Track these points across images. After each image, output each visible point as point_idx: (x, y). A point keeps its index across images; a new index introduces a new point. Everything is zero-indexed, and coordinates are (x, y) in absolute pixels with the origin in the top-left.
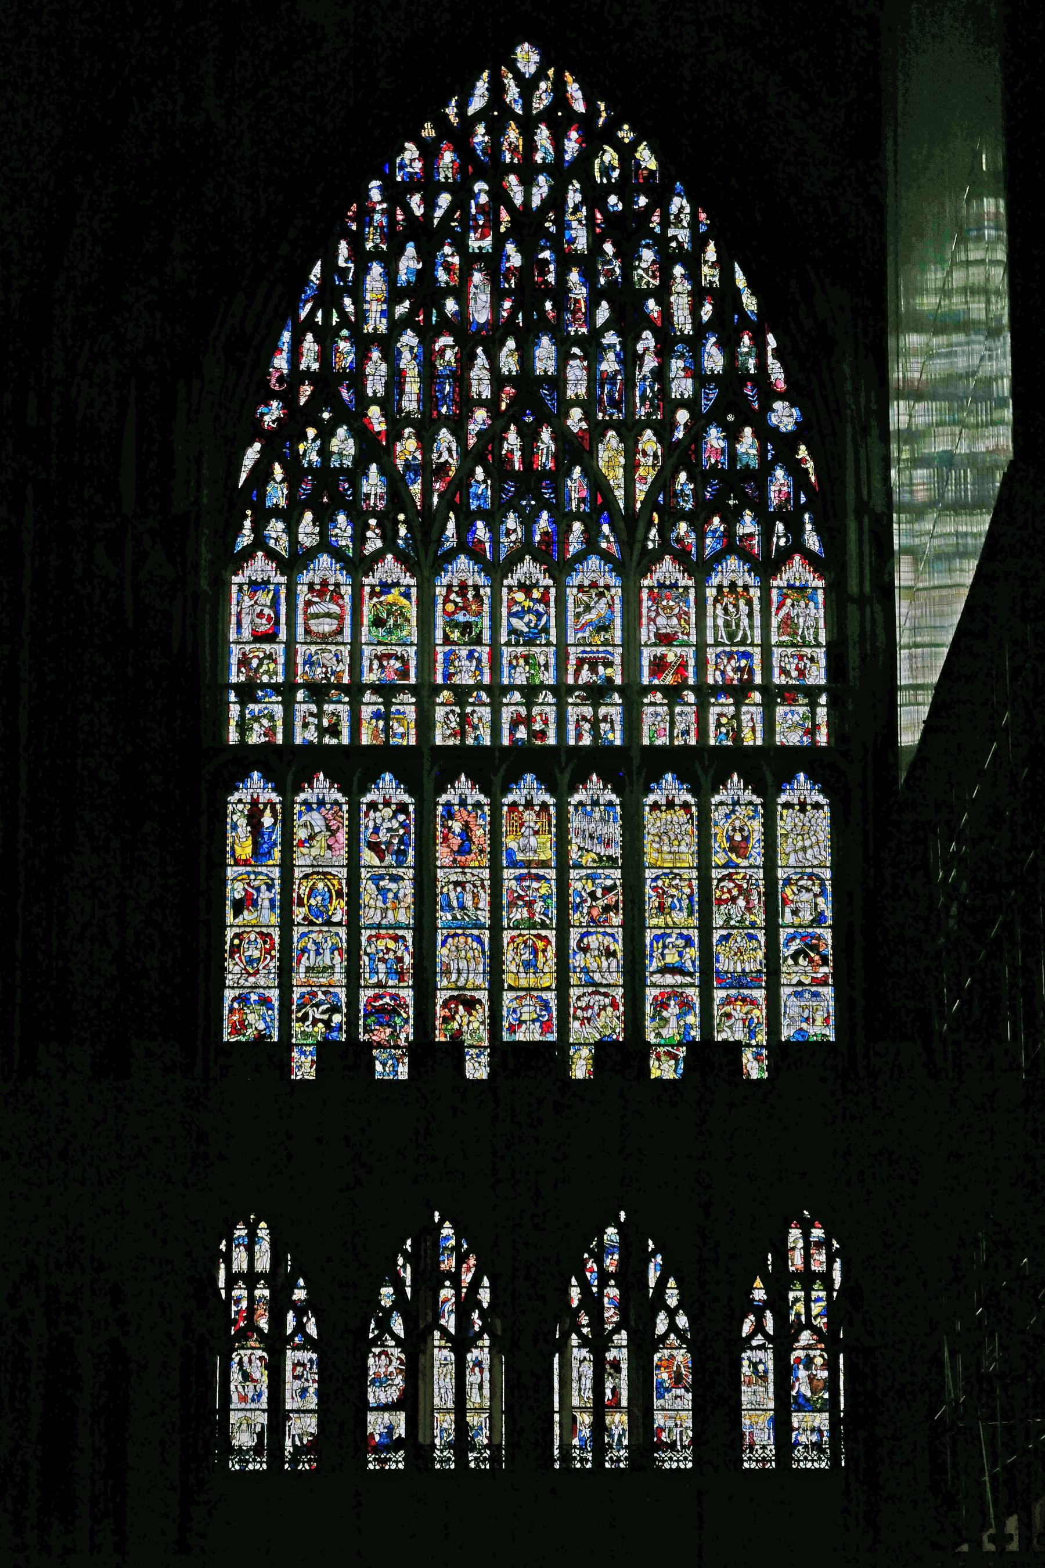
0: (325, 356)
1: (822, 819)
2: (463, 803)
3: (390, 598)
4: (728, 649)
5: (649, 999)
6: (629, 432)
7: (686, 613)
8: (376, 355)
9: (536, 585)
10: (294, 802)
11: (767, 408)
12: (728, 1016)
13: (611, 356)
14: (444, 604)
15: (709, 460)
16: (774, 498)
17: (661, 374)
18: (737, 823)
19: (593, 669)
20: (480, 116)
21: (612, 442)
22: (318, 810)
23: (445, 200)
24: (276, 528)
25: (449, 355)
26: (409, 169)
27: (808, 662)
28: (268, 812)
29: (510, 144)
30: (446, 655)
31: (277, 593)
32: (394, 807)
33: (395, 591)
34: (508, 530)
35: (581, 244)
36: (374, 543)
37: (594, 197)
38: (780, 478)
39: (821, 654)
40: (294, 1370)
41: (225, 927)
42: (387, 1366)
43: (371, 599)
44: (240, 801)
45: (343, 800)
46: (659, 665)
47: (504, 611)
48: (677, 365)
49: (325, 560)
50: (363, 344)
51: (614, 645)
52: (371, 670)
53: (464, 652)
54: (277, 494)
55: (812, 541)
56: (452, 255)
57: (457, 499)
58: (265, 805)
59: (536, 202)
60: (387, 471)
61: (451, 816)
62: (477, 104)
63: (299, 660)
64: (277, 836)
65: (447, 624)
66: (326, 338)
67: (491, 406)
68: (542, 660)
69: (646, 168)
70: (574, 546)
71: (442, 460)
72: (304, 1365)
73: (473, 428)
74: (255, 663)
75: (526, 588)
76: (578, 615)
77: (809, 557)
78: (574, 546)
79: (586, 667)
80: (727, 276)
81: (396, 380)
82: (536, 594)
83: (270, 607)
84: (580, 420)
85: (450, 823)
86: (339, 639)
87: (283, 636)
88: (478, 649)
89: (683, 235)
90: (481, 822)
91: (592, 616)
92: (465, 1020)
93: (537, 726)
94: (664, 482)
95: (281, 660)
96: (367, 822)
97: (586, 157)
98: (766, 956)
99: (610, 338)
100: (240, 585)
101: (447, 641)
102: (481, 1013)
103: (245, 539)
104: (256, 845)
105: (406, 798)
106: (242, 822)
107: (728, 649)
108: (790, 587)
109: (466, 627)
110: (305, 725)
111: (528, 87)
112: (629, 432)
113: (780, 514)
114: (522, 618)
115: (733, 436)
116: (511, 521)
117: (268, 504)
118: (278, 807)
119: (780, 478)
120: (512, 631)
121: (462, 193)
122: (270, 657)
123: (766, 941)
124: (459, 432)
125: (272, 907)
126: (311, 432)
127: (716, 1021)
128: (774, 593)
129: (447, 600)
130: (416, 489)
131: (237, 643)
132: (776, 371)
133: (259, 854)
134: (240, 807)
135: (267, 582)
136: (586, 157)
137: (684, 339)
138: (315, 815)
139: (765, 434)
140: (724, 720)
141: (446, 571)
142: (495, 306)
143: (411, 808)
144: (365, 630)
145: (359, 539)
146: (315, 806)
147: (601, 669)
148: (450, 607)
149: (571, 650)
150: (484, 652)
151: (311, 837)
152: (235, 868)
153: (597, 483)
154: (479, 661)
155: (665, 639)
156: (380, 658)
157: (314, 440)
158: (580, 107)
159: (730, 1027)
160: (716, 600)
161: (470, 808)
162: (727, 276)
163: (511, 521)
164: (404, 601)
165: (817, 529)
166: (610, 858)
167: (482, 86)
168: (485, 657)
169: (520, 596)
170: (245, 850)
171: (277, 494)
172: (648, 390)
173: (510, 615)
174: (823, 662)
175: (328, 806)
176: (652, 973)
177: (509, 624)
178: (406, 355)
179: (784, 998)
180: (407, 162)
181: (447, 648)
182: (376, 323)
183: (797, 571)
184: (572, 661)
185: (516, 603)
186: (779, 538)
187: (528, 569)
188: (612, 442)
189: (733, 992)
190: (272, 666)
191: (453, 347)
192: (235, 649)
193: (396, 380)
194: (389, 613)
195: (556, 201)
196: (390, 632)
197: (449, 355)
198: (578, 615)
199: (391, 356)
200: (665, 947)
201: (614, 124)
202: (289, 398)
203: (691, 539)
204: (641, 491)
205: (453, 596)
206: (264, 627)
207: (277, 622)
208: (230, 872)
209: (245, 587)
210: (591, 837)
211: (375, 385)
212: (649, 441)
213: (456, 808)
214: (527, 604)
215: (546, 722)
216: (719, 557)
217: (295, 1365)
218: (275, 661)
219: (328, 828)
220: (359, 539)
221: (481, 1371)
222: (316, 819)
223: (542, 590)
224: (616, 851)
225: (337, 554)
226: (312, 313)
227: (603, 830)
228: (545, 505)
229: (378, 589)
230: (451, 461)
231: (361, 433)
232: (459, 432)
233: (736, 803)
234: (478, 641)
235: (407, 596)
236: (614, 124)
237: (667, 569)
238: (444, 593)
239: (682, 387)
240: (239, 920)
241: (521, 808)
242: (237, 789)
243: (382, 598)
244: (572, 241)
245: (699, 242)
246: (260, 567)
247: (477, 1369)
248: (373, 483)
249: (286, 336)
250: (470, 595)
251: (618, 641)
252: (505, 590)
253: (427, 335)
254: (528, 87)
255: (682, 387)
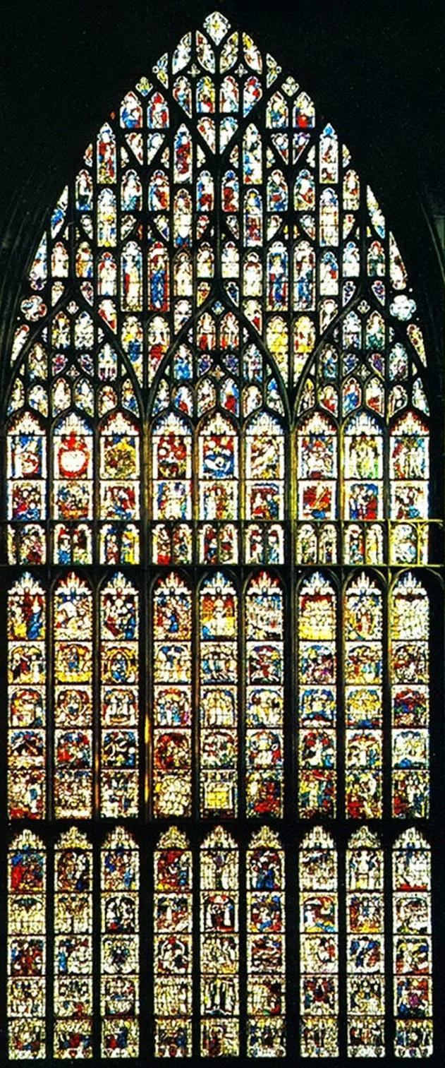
0: (72, 262)
1: (423, 606)
2: (172, 594)
3: (119, 446)
4: (359, 483)
5: (302, 738)
6: (290, 318)
7: (330, 457)
8: (108, 263)
9: (224, 435)
10: (54, 595)
11: (390, 300)
12: (355, 748)
13: (277, 261)
14: (159, 449)
15: (348, 340)
16: (394, 370)
17: (314, 279)
18: (363, 611)
19: (264, 498)
20: (183, 73)
21: (278, 325)
22: (71, 601)
23: (157, 141)
24: (38, 395)
25: (161, 262)
26: (130, 118)
27: (416, 492)
28: (36, 603)
29: (205, 96)
30: (161, 487)
31: (39, 442)
32: (123, 598)
33: (123, 440)
34: (203, 395)
35: (257, 177)
36: (108, 405)
37: (267, 137)
38: (398, 352)
39: (424, 486)
40: (60, 989)
41: (8, 684)
42: (122, 987)
43: (106, 447)
44: (16, 594)
45: (89, 593)
46: (310, 496)
47: (201, 454)
48: (324, 270)
49: (73, 418)
50: (97, 251)
51: (279, 479)
52: (105, 499)
53: (172, 485)
54: (39, 370)
55: (421, 403)
56: (162, 186)
57: (167, 372)
58: (34, 596)
59: (224, 142)
60: (117, 348)
61: (164, 604)
62: (180, 64)
63: (56, 491)
64: (43, 620)
65: (161, 465)
66: (71, 248)
67: (192, 300)
68: (229, 492)
69: (304, 115)
70: (251, 405)
71: (157, 342)
72: (66, 986)
73: (178, 318)
74: (25, 494)
75: (216, 437)
76: (253, 459)
77: (418, 414)
78: (251, 405)
79: (259, 495)
80: (363, 201)
81: (122, 281)
82: (224, 442)
83: (35, 454)
84: (256, 312)
85: (163, 609)
86: (84, 476)
87: (44, 475)
88: (183, 482)
89: (333, 168)
90: (185, 609)
91: (264, 459)
92: (176, 751)
93: (226, 539)
94: (313, 358)
95: (43, 492)
96: (106, 608)
97: (260, 108)
98: (383, 705)
99: (278, 248)
100: (14, 437)
101: (161, 476)
102: (187, 745)
103: (17, 404)
104: (29, 627)
105: (133, 591)
106: (18, 611)
107: (359, 483)
108: (404, 435)
109: (174, 467)
110: (61, 541)
111: (217, 51)
112: (290, 318)
113: (399, 381)
114: (214, 460)
115: (364, 319)
116: (206, 388)
117: (32, 376)
118: (43, 598)
119: (398, 352)
120: (207, 470)
121: (169, 134)
122: (35, 490)
123: (383, 696)
124: (169, 318)
125: (41, 671)
126: (62, 322)
127: (347, 752)
128: (392, 440)
129: (160, 447)
130: (137, 364)
131: (12, 479)
132: (397, 274)
133: (31, 635)
134: (17, 599)
135: (33, 434)
136: (260, 108)
137: (331, 249)
138: (68, 604)
139: (390, 321)
140: (355, 536)
141: (160, 425)
142: (194, 225)
143: (136, 599)
144: (102, 470)
145: (97, 401)
146: (69, 598)
147: (269, 497)
148: (163, 452)
149: (248, 483)
150: (186, 484)
151: (67, 620)
152: (14, 643)
153: (268, 358)
154: (184, 491)
155: (316, 476)
156: (111, 490)
157: (64, 328)
158: (255, 65)
159: (357, 755)
160: (352, 447)
161: (178, 598)
162: (363, 201)
163: (206, 388)
164: (129, 448)
165: (425, 391)
166: (274, 634)
167: (183, 50)
168: (188, 489)
169: (212, 444)
170: (21, 630)
171: (39, 370)
172: (305, 288)
173: (205, 457)
174: (426, 492)
175: (78, 598)
176: (304, 720)
177: (204, 464)
178: (130, 264)
179: (394, 737)
180: (129, 111)
181: (161, 482)
182: (107, 239)
183: (410, 425)
184: (249, 491)
185: (209, 449)
186: (397, 401)
187: (219, 424)
188: (278, 325)
189: (360, 732)
190: (37, 497)
191: (163, 256)
192: (10, 483)
193: (122, 281)
194: (121, 457)
195: (237, 139)
196: (120, 471)
197: (161, 262)
198: (253, 459)
199: (118, 263)
200: (313, 700)
201: (281, 80)
202: (46, 296)
203: (334, 402)
204: (299, 364)
205: (165, 445)
206: (30, 469)
207: (40, 465)
208: (11, 645)
209: (17, 438)
210: (262, 619)
211: (108, 288)
212: (304, 325)
213: (168, 598)
214: (218, 450)
215: (231, 537)
216: (352, 416)
217: (61, 986)
218: (39, 493)
219: (79, 615)
220: (97, 401)
221: (187, 992)
222: (70, 608)
223: (228, 439)
224: (279, 630)
225: (82, 414)
226: (62, 231)
227: (271, 614)
228: (229, 375)
229: (110, 439)
230: (162, 343)
231: (98, 321)
232: (169, 318)
233: (363, 595)
234: (183, 477)
235: (132, 444)
236: (281, 80)
237: (316, 424)
238: (158, 442)
239: (329, 287)
240: (17, 681)
241: (213, 598)
242: (14, 586)
243: (114, 446)
244: (250, 172)
245: (342, 172)
246: (28, 424)
247: (184, 990)
248: (107, 360)
249: (42, 249)
250: (176, 443)
251: (282, 477)
252: (201, 439)
253: (145, 247)
254: (217, 51)
255: (329, 287)
